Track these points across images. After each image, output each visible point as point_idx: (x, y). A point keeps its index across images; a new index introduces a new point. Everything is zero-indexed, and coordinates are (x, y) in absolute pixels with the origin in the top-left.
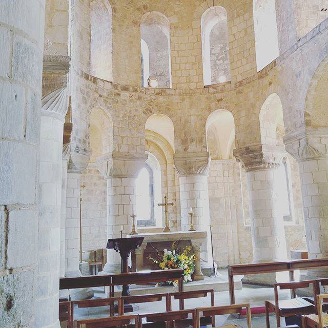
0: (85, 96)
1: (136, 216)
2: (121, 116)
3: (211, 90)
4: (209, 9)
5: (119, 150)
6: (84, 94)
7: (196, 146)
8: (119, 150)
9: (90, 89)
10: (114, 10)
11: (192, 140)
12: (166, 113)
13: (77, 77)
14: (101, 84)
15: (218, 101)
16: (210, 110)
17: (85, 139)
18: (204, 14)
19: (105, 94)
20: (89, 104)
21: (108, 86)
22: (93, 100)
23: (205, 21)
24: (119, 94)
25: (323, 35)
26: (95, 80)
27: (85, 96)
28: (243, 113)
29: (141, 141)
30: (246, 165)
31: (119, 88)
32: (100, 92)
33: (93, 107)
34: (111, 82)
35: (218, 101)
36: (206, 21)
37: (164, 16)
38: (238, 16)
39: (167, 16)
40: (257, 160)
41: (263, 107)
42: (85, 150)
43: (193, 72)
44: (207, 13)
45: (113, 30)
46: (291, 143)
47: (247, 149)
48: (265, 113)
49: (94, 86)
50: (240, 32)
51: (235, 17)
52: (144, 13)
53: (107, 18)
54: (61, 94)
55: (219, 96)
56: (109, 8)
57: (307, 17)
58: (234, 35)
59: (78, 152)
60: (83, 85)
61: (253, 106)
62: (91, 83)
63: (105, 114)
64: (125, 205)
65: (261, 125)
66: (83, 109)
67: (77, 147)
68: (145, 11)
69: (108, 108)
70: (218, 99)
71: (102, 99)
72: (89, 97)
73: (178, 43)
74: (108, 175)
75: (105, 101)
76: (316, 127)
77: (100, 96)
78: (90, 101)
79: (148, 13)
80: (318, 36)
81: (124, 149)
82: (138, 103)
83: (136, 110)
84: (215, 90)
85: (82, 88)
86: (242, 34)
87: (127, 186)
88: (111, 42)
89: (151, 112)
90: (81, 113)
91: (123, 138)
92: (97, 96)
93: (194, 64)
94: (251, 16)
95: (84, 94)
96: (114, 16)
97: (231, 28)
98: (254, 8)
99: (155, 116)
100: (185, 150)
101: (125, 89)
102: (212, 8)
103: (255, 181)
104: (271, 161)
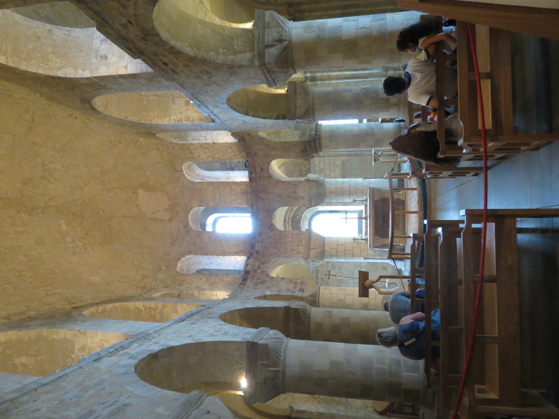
0: (260, 281)
1: (354, 238)
2: (275, 250)
3: (253, 175)
4: (186, 175)
5: (302, 253)
6: (258, 283)
7: (300, 189)
8: (302, 253)
9: (254, 276)
10: (190, 253)
11: (295, 192)
12: (273, 213)
13: (245, 288)
14: (249, 267)
15: (262, 170)
16: (270, 177)
17: (293, 283)
18: (189, 178)
19: (257, 263)
20: (267, 279)
21: (251, 260)
22: (263, 274)
23: (195, 177)
24: (257, 252)
25: (213, 110)
26: (247, 272)
27: (260, 281)
28: (273, 153)
29: (295, 235)
30: (317, 152)
31: (252, 251)
32: (256, 268)
33: (268, 274)
34: (248, 258)
35: (262, 170)
36: (195, 176)
37: (192, 211)
38: (192, 153)
39: (192, 209)
40: (312, 144)
41: (269, 138)
42: (302, 283)
43: (238, 189)
44: (189, 175)
45: (206, 254)
46: (300, 127)
47: (303, 151)
48: (273, 136)
49: (252, 274)
50: (205, 153)
51: (192, 156)
52: (190, 227)
53: (196, 258)
54: (274, 347)
55: (258, 169)
56: (188, 257)
57: (196, 112)
58: (208, 157)
59: (304, 289)
60: (251, 283)
61: (267, 146)
62: (250, 275)
63: (274, 262)
64: (345, 249)
65: (282, 140)
66: (270, 284)
67: (300, 290)
68: (189, 227)
69: (269, 261)
70: (260, 171)
71: (261, 266)
72: (260, 278)
73: (214, 201)
74: (321, 261)
75: (263, 263)
76: (289, 111)
77: (259, 267)
78: (264, 277)
79: (190, 224)
80: (215, 112)
81: (302, 249)
82: (264, 236)
83: (270, 238)
84: (254, 173)
85: (254, 284)
86: (207, 151)
87: (331, 247)
88: (215, 257)
89: (271, 225)
90: (273, 286)
91: (292, 250)
92: (259, 271)
93: (231, 188)
94: (193, 144)
95: (258, 283)
96: (195, 253)
97: (202, 159)
98: (184, 142)
99: (274, 222)
100: (303, 198)
101: (253, 246)
102: (184, 172)
103: (329, 146)
104: (313, 132)
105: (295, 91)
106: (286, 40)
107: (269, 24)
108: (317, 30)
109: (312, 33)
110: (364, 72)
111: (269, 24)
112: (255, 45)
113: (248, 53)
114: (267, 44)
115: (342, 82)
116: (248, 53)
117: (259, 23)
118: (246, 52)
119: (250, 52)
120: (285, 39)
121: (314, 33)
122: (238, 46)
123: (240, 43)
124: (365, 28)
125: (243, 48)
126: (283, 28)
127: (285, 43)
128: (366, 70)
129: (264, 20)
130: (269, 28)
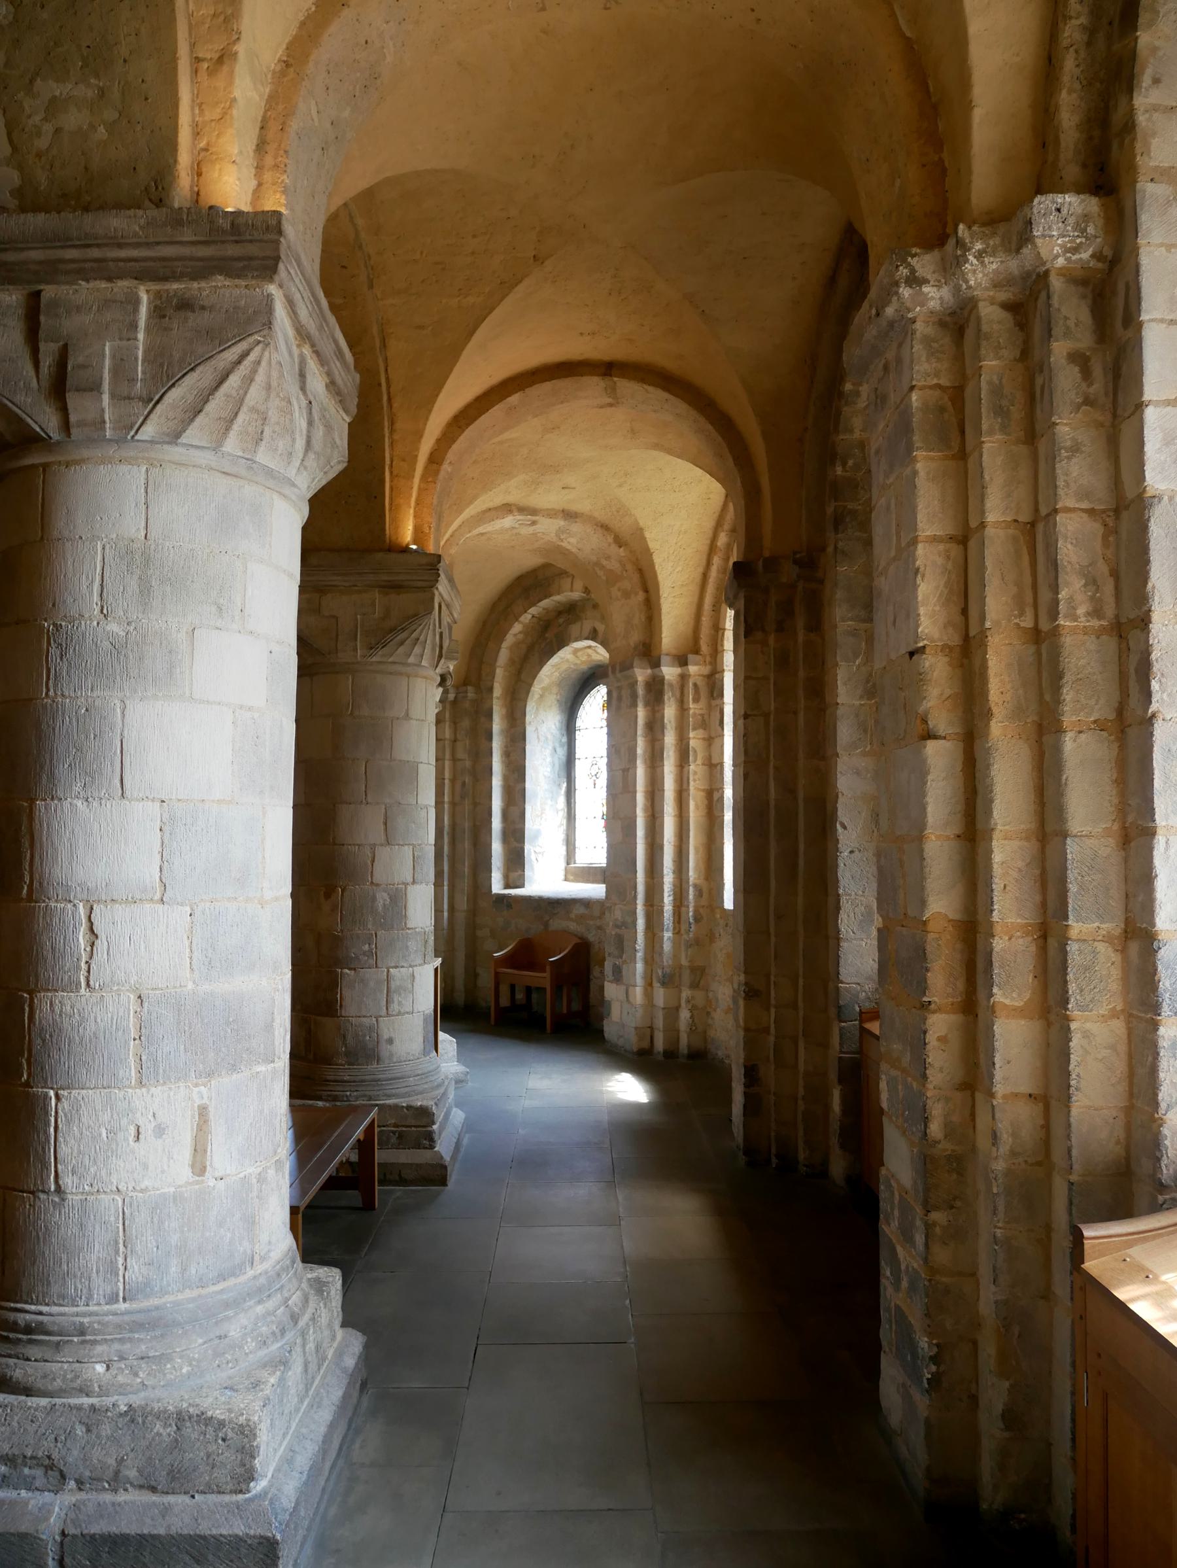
105: (396, 587)
106: (66, 426)
107: (185, 305)
108: (113, 627)
109: (96, 598)
110: (666, 894)
111: (185, 305)
112: (41, 217)
113: (15, 178)
114: (49, 292)
115: (635, 806)
116: (15, 178)
117: (188, 237)
118: (20, 168)
119: (18, 193)
120: (73, 418)
121: (97, 610)
122: (54, 107)
123: (73, 119)
124: (92, 945)
125: (42, 143)
126: (152, 401)
127: (46, 420)
128: (675, 900)
129: (204, 270)
130: (158, 313)
